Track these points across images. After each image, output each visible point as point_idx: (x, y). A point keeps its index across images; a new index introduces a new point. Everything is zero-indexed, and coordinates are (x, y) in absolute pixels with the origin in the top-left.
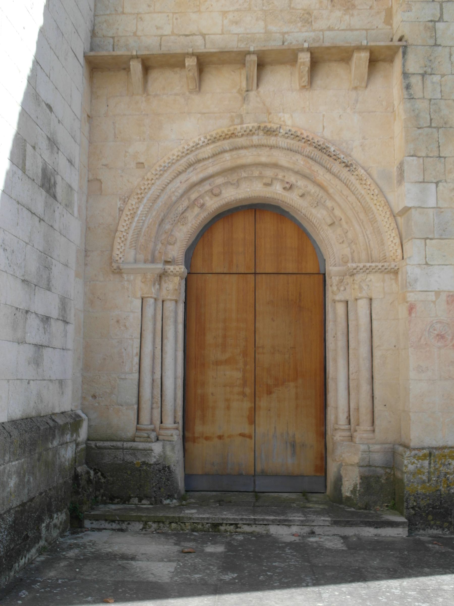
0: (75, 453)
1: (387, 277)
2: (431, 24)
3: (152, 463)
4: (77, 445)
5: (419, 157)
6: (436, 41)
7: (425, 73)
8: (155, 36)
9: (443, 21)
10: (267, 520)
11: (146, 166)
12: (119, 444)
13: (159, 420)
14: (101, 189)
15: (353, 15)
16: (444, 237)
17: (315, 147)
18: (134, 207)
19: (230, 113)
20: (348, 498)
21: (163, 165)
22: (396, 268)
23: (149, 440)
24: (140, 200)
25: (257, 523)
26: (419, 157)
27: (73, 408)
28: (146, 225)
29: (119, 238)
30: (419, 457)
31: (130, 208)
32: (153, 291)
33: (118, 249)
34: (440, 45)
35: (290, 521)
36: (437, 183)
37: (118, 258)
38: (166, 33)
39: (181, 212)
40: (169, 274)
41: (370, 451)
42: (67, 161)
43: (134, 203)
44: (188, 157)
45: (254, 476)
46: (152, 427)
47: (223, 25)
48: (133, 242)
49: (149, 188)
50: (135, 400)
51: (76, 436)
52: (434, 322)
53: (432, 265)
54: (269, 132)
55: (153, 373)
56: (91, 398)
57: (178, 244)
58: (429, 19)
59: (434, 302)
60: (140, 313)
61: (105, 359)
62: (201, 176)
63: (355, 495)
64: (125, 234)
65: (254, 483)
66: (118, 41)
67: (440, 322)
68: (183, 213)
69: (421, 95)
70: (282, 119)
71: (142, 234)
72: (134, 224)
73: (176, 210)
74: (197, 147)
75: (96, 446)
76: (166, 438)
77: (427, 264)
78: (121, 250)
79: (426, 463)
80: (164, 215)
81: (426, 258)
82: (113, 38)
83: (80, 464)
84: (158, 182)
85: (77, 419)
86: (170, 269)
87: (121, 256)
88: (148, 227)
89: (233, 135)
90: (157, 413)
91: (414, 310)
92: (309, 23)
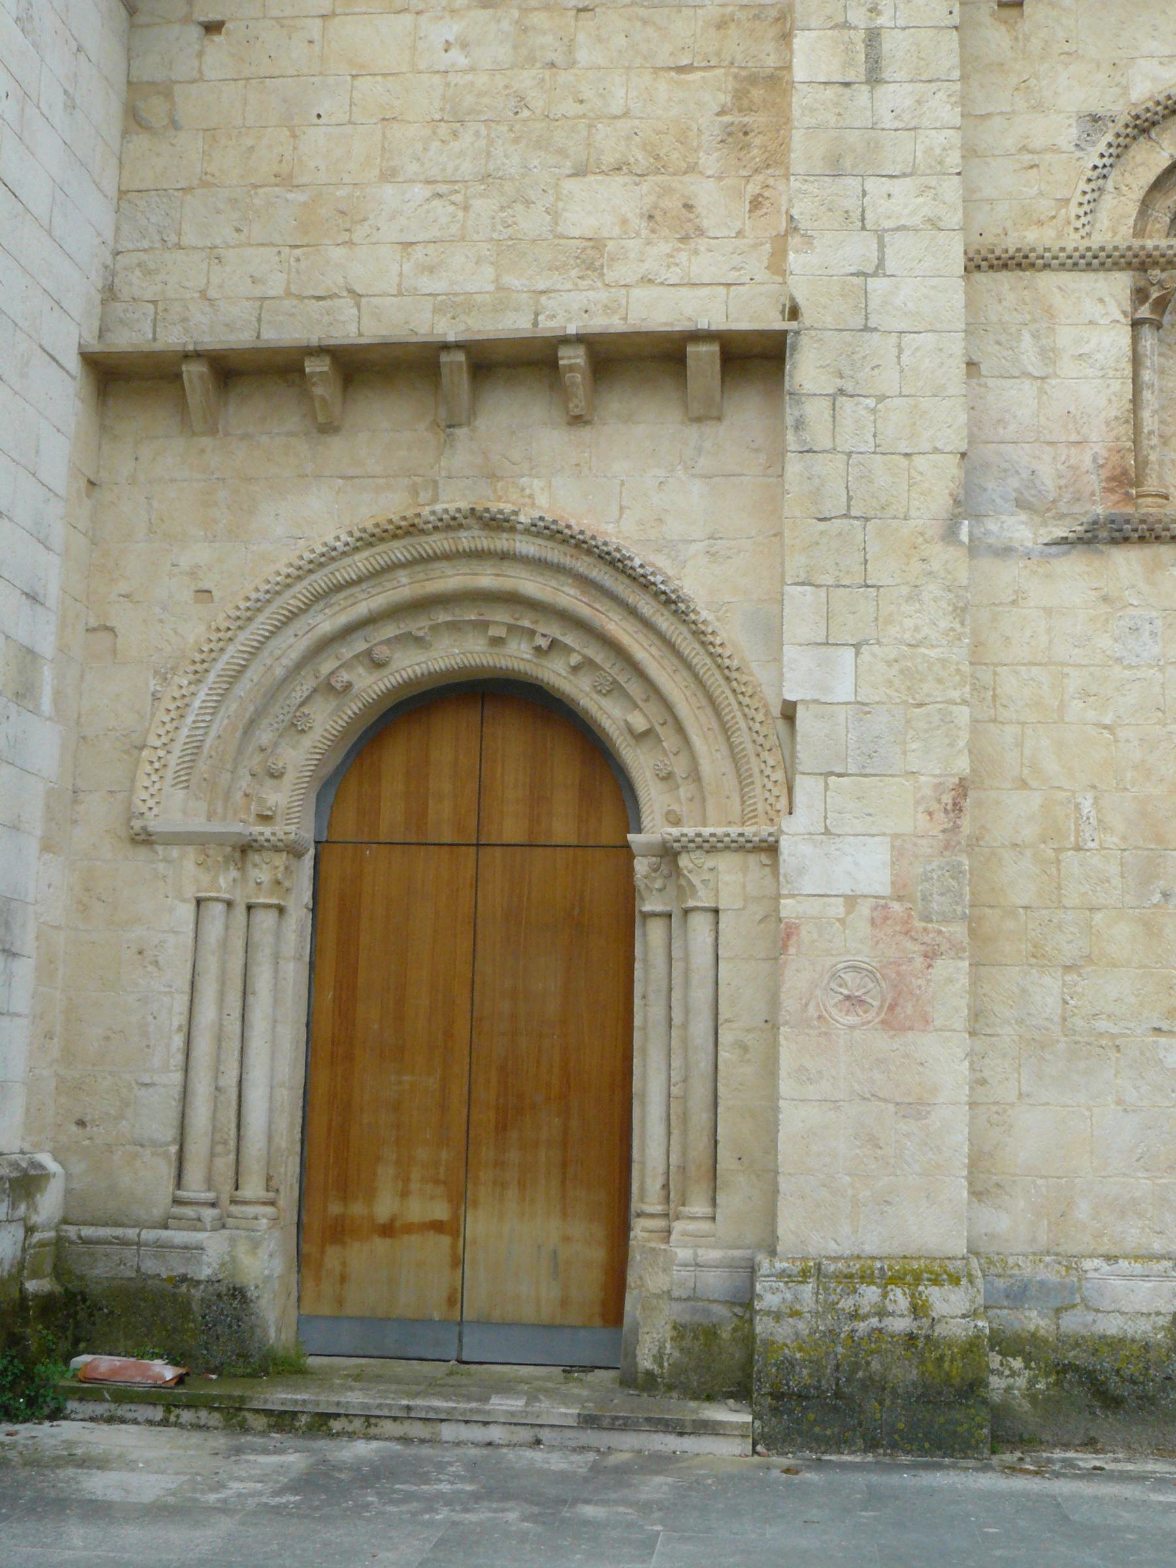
0: (24, 1250)
1: (752, 859)
2: (855, 280)
3: (202, 1278)
4: (30, 1230)
5: (818, 586)
6: (867, 319)
7: (841, 392)
8: (248, 299)
9: (885, 275)
10: (435, 1410)
11: (216, 599)
12: (131, 1233)
13: (232, 1182)
14: (114, 652)
15: (696, 252)
16: (868, 771)
17: (600, 557)
18: (184, 692)
19: (409, 476)
20: (649, 1374)
21: (254, 596)
22: (771, 839)
23: (199, 1224)
24: (198, 678)
25: (413, 1415)
26: (818, 586)
27: (27, 1147)
28: (213, 733)
29: (147, 764)
30: (789, 1276)
31: (177, 694)
32: (223, 885)
33: (146, 788)
34: (875, 330)
35: (488, 1412)
36: (857, 647)
37: (144, 809)
38: (271, 293)
39: (299, 700)
40: (262, 846)
41: (697, 1265)
42: (24, 597)
43: (185, 682)
44: (313, 577)
45: (461, 1323)
46: (211, 1196)
47: (401, 275)
48: (182, 773)
49: (222, 650)
50: (170, 1133)
51: (28, 1209)
52: (841, 966)
53: (839, 835)
54: (497, 523)
55: (217, 1073)
56: (74, 1128)
58: (853, 269)
59: (842, 921)
60: (191, 934)
61: (107, 1038)
62: (343, 619)
63: (661, 1366)
64: (161, 753)
65: (460, 1341)
66: (166, 310)
67: (855, 969)
68: (302, 704)
69: (828, 445)
70: (528, 492)
71: (205, 751)
72: (185, 731)
73: (288, 697)
74: (330, 557)
75: (80, 1237)
76: (243, 1223)
77: (827, 832)
78: (152, 790)
79: (808, 1289)
80: (256, 710)
81: (826, 818)
82: (154, 302)
83: (36, 1274)
84: (242, 636)
85: (33, 1172)
86: (262, 834)
87: (151, 803)
88: (219, 737)
89: (410, 529)
90: (224, 1164)
91: (794, 939)
92: (595, 270)
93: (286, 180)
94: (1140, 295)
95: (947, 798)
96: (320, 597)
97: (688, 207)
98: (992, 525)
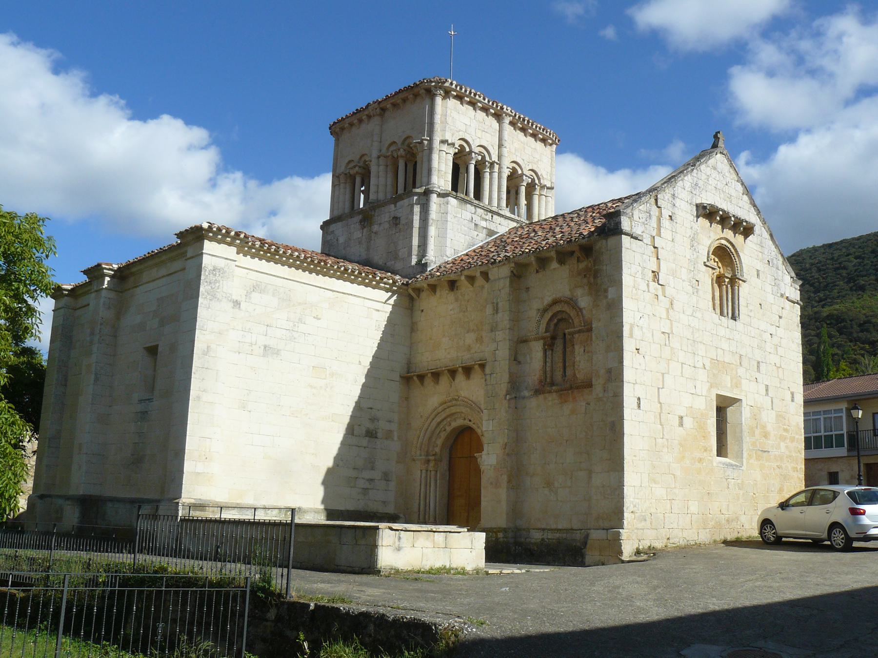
2: (494, 352)
27: (396, 512)
54: (456, 400)
57: (438, 447)
59: (489, 469)
69: (489, 383)
93: (431, 339)
94: (544, 345)
95: (504, 447)
96: (436, 416)
97: (482, 337)
98: (522, 393)
